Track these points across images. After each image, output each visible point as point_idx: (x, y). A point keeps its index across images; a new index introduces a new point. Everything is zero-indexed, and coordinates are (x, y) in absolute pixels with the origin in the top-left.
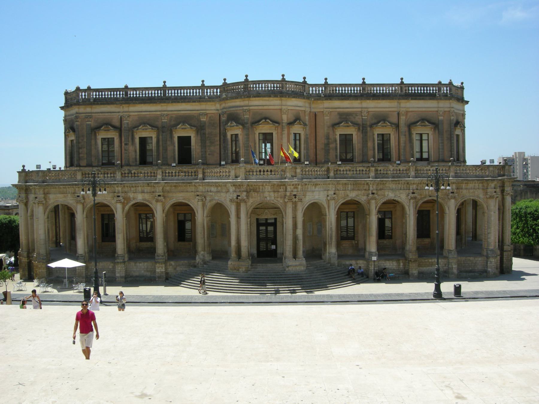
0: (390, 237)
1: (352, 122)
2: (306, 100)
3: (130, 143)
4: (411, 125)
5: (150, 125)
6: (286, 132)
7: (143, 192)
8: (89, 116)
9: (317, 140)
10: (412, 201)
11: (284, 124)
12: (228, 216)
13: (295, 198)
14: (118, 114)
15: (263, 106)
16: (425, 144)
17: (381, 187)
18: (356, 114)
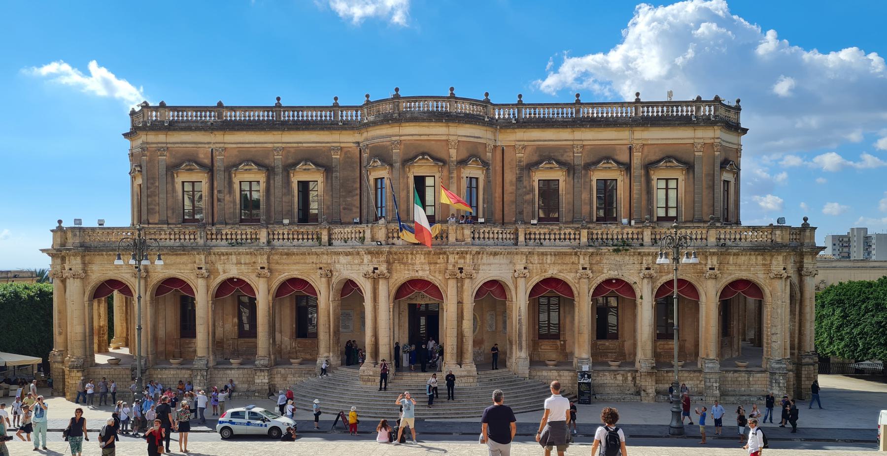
0: (615, 337)
1: (558, 162)
2: (488, 128)
3: (226, 190)
4: (649, 166)
5: (256, 164)
6: (455, 175)
7: (239, 263)
8: (164, 149)
10: (646, 281)
12: (362, 299)
13: (461, 272)
14: (207, 146)
15: (420, 135)
16: (672, 194)
17: (598, 258)
18: (564, 149)
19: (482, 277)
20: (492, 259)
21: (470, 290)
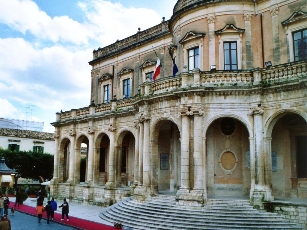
9: (265, 46)
11: (210, 34)
13: (189, 110)
19: (213, 114)
20: (221, 99)
21: (200, 127)
